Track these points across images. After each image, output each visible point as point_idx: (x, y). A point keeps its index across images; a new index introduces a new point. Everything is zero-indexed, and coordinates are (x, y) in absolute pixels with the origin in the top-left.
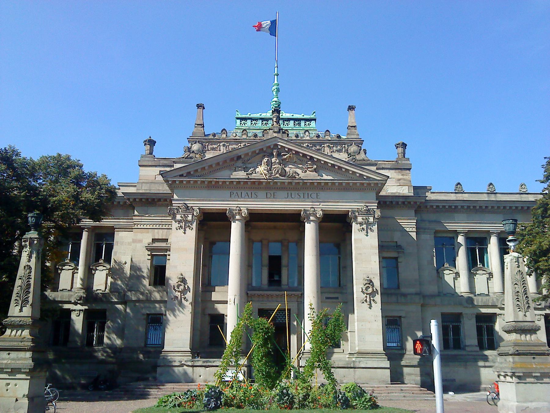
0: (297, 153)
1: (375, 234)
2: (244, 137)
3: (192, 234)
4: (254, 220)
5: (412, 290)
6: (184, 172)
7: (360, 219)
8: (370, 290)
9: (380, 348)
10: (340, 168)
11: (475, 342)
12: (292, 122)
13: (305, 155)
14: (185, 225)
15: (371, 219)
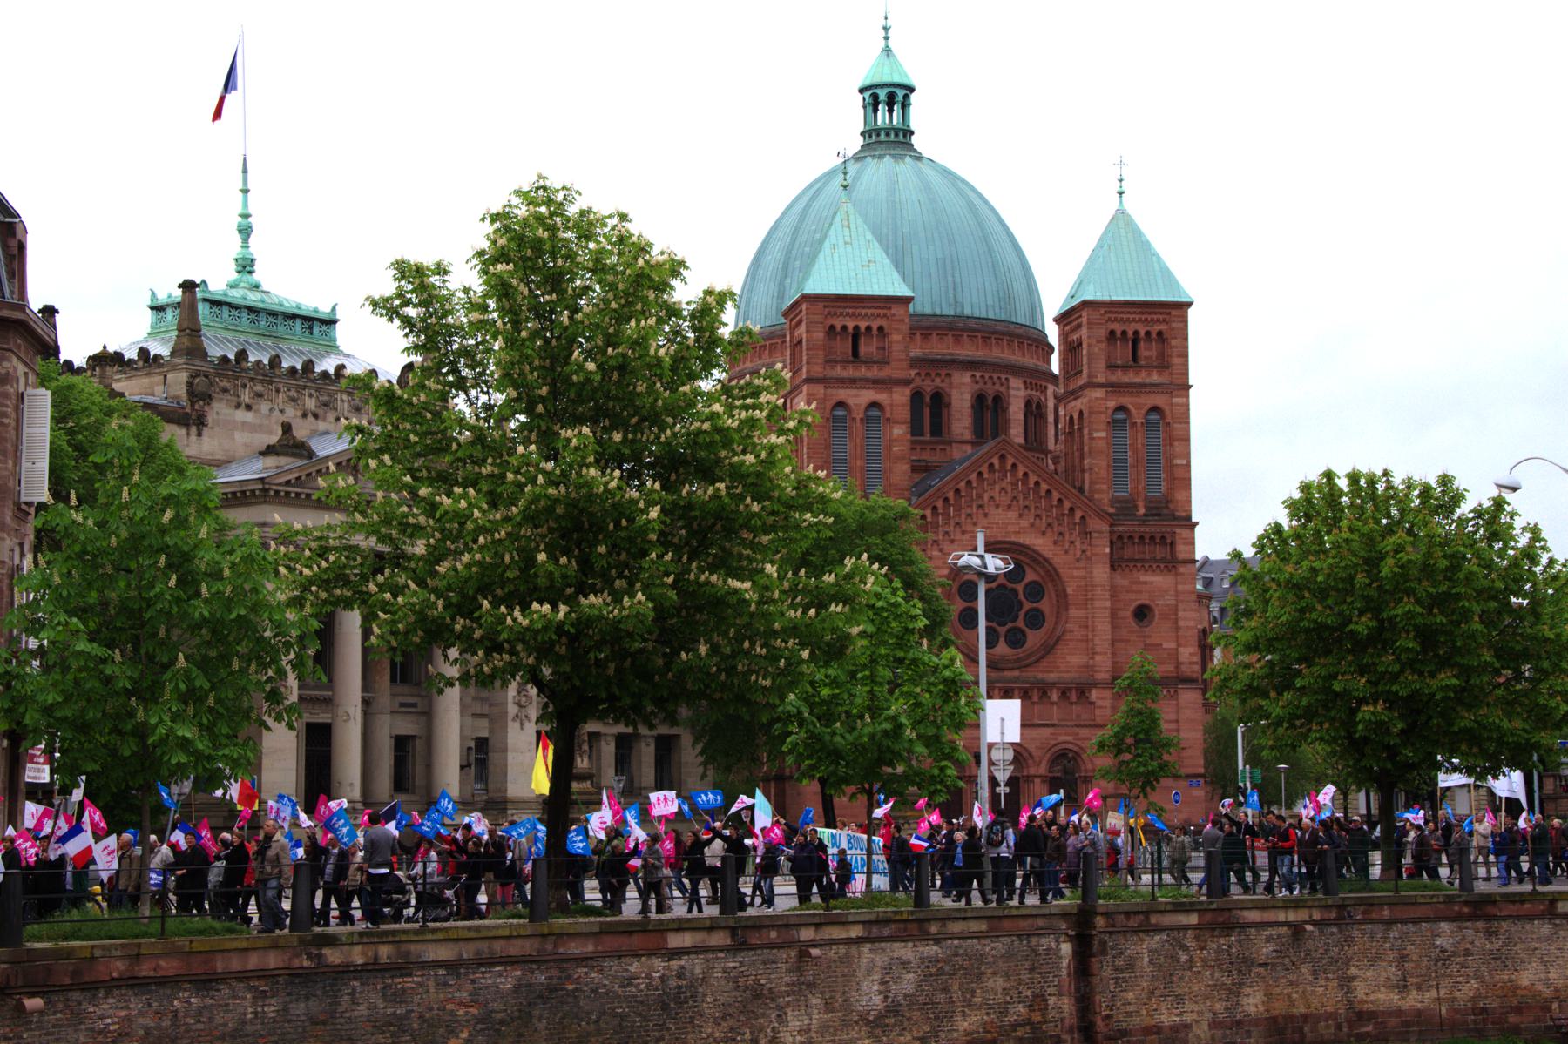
12: (298, 322)
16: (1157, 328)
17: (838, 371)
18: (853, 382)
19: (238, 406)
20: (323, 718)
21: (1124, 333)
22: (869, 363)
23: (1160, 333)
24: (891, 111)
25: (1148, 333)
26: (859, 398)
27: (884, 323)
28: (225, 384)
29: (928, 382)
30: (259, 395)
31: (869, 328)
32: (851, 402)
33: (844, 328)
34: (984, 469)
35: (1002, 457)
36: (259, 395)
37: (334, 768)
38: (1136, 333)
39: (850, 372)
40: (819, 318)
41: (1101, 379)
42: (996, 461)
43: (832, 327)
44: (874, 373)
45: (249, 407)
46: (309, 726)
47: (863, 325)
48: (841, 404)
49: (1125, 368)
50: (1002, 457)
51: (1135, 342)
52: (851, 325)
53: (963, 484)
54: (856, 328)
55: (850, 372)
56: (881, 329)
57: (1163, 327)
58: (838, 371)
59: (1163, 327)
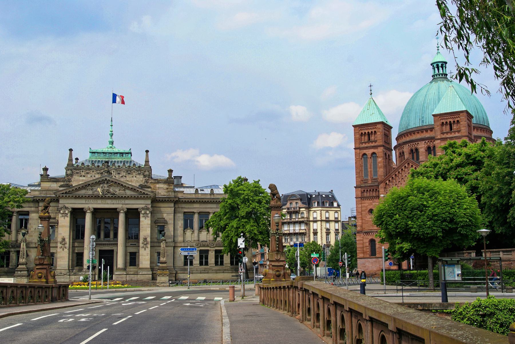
0: (116, 182)
1: (149, 218)
2: (93, 167)
4: (96, 212)
5: (170, 240)
6: (64, 192)
7: (143, 212)
8: (145, 243)
10: (135, 189)
11: (198, 262)
12: (119, 154)
13: (119, 184)
15: (148, 212)
16: (457, 119)
17: (364, 145)
18: (366, 148)
19: (81, 176)
21: (446, 122)
22: (372, 142)
23: (458, 121)
24: (438, 70)
25: (454, 122)
26: (369, 152)
27: (376, 130)
28: (78, 171)
29: (431, 143)
30: (88, 173)
31: (372, 132)
32: (367, 153)
33: (365, 133)
34: (403, 168)
35: (408, 164)
36: (88, 173)
37: (137, 260)
38: (450, 122)
40: (357, 131)
41: (439, 137)
42: (406, 165)
43: (362, 133)
44: (373, 144)
45: (84, 176)
46: (100, 251)
47: (370, 131)
48: (365, 154)
49: (447, 133)
50: (408, 164)
51: (451, 125)
52: (367, 132)
53: (397, 173)
54: (368, 132)
56: (375, 132)
58: (364, 145)
59: (458, 119)
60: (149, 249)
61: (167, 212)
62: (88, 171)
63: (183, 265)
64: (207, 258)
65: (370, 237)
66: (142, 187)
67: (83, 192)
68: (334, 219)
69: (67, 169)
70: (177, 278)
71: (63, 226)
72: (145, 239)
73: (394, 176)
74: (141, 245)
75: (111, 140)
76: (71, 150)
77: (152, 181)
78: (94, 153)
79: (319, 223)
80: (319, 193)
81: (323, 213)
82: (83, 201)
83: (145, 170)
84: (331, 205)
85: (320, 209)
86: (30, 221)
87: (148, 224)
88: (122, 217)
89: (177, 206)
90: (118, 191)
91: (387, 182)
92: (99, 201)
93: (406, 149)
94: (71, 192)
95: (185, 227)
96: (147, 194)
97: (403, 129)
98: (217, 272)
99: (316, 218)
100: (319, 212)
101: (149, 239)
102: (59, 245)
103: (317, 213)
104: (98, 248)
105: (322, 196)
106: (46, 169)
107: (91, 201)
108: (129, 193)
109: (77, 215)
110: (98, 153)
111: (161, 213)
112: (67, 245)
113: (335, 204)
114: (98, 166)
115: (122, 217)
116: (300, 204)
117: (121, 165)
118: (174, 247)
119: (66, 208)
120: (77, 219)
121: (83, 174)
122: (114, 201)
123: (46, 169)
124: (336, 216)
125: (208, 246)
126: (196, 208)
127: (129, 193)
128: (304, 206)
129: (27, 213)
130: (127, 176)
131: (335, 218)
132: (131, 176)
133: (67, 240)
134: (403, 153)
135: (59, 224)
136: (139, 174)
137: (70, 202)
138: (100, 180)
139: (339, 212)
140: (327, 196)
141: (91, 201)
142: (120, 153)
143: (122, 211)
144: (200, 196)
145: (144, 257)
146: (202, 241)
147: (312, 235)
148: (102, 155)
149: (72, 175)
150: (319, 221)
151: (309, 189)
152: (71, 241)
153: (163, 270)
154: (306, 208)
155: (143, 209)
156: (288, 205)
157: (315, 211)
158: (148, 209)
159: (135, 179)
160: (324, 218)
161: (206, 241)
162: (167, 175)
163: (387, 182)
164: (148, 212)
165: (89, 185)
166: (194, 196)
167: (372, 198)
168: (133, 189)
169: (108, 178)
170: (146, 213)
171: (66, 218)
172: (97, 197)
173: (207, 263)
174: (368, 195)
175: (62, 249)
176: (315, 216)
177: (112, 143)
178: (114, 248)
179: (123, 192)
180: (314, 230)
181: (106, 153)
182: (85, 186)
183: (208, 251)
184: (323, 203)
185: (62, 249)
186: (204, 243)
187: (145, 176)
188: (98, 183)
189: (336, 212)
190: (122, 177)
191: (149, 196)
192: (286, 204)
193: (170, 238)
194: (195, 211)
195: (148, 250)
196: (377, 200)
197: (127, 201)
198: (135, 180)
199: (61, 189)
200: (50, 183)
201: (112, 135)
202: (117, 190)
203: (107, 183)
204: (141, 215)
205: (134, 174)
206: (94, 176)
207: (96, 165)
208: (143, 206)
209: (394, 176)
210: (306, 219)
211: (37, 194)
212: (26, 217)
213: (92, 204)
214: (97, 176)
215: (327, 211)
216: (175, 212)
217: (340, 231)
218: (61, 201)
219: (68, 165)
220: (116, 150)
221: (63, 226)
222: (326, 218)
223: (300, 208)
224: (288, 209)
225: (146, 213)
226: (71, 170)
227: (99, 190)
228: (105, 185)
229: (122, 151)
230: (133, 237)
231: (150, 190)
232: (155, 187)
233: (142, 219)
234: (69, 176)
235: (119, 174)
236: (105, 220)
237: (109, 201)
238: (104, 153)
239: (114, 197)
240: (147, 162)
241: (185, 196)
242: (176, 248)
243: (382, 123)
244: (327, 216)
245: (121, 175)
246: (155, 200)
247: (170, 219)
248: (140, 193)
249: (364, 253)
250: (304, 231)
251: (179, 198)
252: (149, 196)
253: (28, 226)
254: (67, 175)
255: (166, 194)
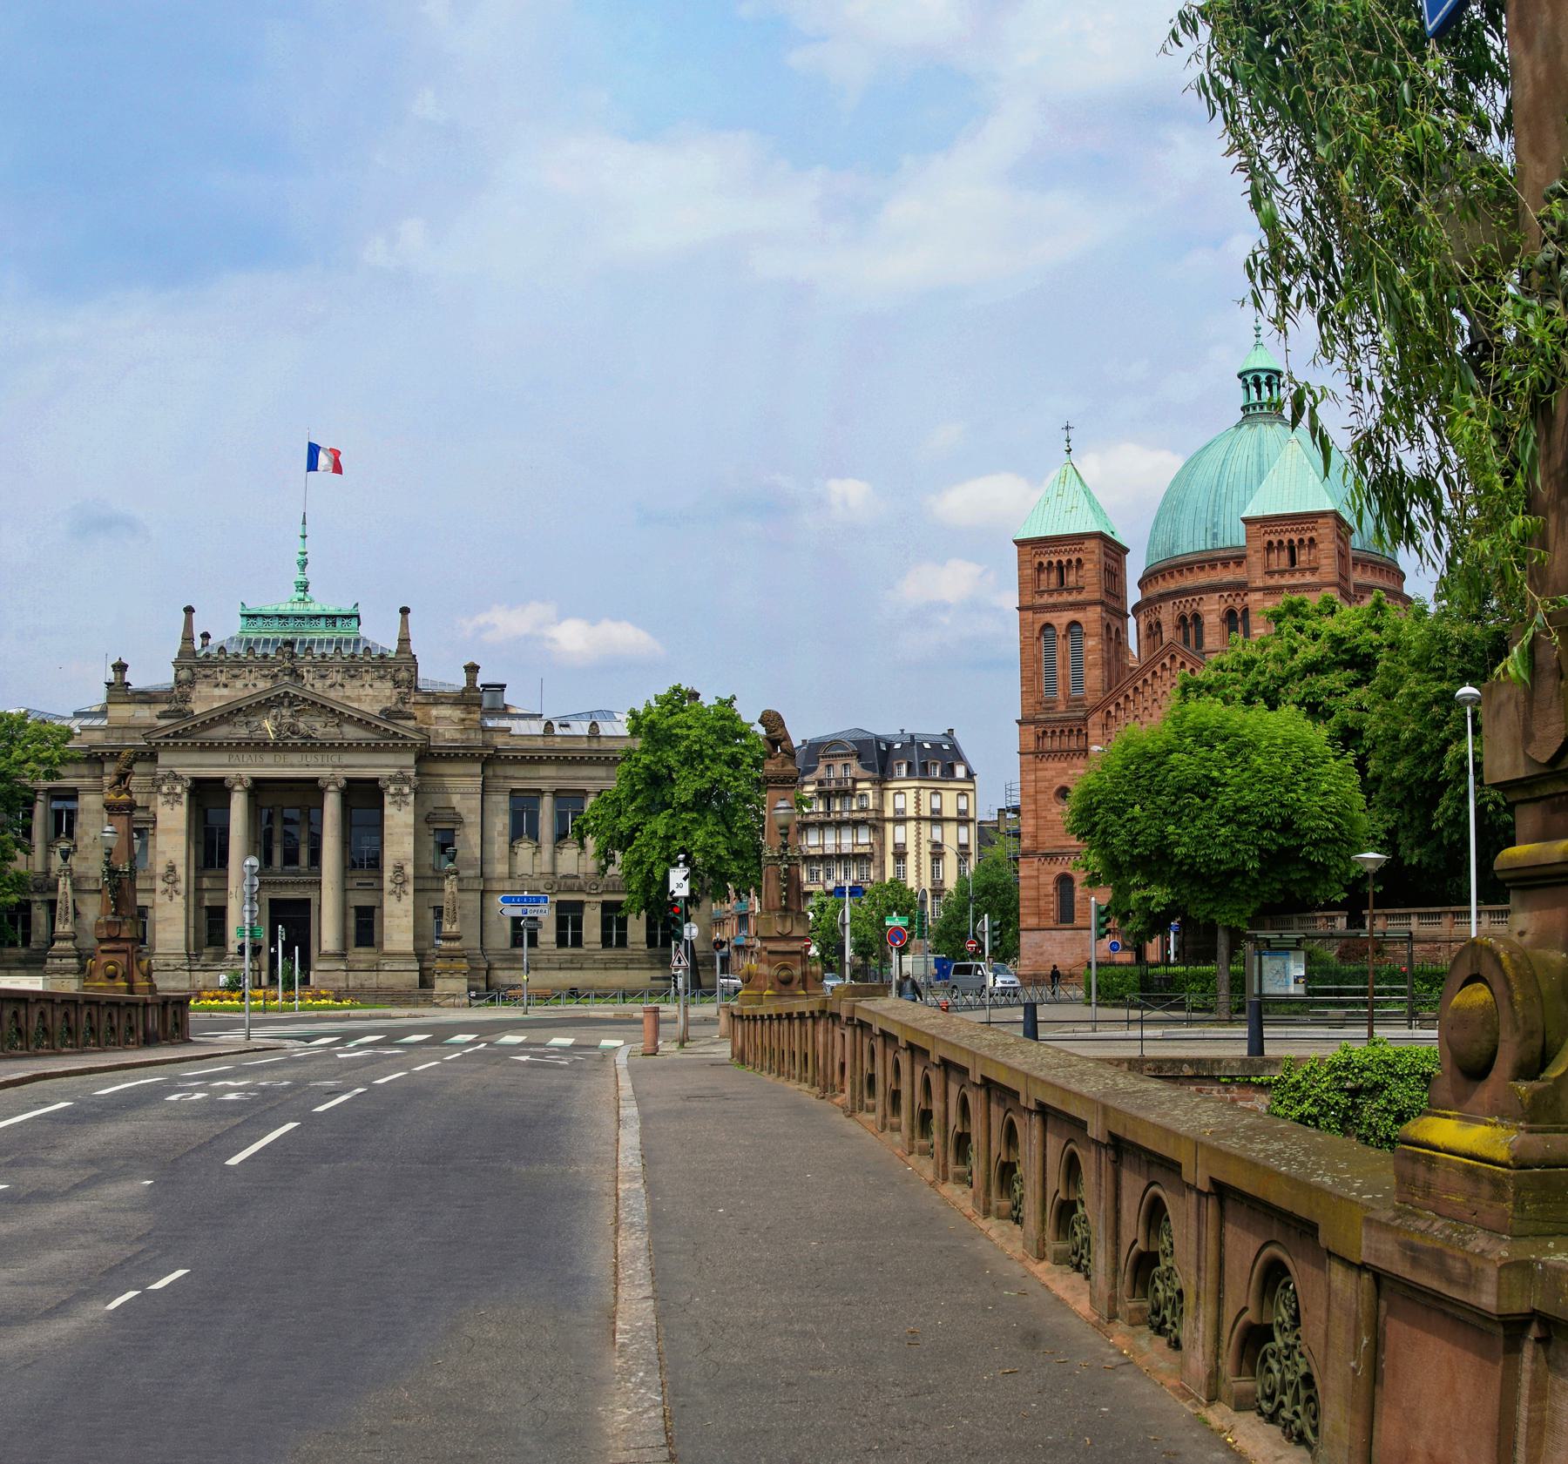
0: (314, 703)
1: (411, 808)
3: (181, 811)
4: (258, 788)
7: (392, 790)
9: (410, 948)
10: (368, 723)
11: (553, 938)
12: (323, 621)
14: (173, 798)
15: (406, 790)
18: (1054, 607)
19: (217, 686)
20: (51, 896)
22: (1070, 590)
26: (1061, 619)
27: (1081, 555)
28: (208, 672)
30: (235, 676)
31: (1069, 561)
32: (1054, 622)
33: (1050, 563)
34: (1158, 668)
36: (235, 676)
37: (376, 929)
39: (1055, 599)
40: (1027, 558)
43: (1041, 564)
45: (226, 686)
46: (271, 901)
47: (1064, 559)
48: (1048, 626)
52: (1055, 561)
54: (1060, 562)
55: (1055, 599)
56: (1079, 561)
57: (1314, 534)
58: (1047, 599)
60: (411, 897)
61: (461, 790)
62: (236, 672)
63: (508, 945)
64: (578, 925)
65: (1058, 869)
66: (389, 714)
67: (221, 732)
68: (954, 815)
69: (179, 665)
70: (492, 982)
71: (168, 831)
72: (399, 869)
73: (1130, 692)
74: (388, 886)
75: (300, 578)
76: (189, 610)
77: (419, 698)
78: (254, 616)
79: (912, 825)
80: (912, 737)
81: (925, 794)
82: (223, 758)
83: (399, 667)
84: (949, 773)
85: (916, 784)
86: (81, 817)
87: (406, 826)
88: (331, 805)
89: (490, 772)
90: (320, 728)
91: (1112, 708)
92: (269, 758)
93: (1167, 614)
94: (189, 732)
95: (515, 835)
96: (404, 737)
97: (1160, 557)
98: (607, 966)
99: (903, 811)
100: (911, 794)
101: (409, 870)
102: (160, 885)
103: (905, 796)
104: (267, 895)
105: (921, 745)
106: (120, 668)
107: (246, 757)
108: (351, 733)
109: (207, 797)
110: (264, 616)
111: (444, 791)
112: (182, 886)
113: (960, 772)
114: (265, 656)
115: (331, 805)
116: (855, 768)
117: (330, 651)
118: (483, 893)
119: (177, 778)
120: (206, 811)
121: (222, 679)
122: (311, 758)
123: (120, 668)
124: (963, 806)
125: (581, 890)
126: (547, 778)
127: (351, 733)
128: (869, 774)
129: (73, 794)
130: (346, 682)
131: (960, 812)
132: (359, 683)
133: (181, 871)
134: (1159, 625)
135: (159, 825)
136: (381, 678)
137: (188, 762)
138: (271, 695)
139: (971, 795)
140: (936, 747)
141: (246, 756)
142: (328, 617)
143: (332, 788)
144: (558, 743)
145: (397, 921)
146: (565, 877)
147: (889, 860)
148: (276, 622)
149: (191, 683)
150: (911, 819)
151: (885, 725)
152: (192, 874)
153: (452, 958)
154: (873, 781)
155: (392, 779)
156: (821, 772)
157: (900, 791)
158: (405, 780)
159: (369, 691)
160: (926, 812)
161: (576, 877)
162: (461, 681)
163: (1112, 708)
164: (406, 790)
165: (240, 710)
166: (540, 743)
167: (1067, 754)
168: (362, 722)
169: (292, 691)
170: (400, 793)
171: (177, 807)
172: (262, 746)
173: (578, 941)
174: (1056, 745)
175: (166, 897)
176: (900, 805)
177: (304, 587)
178: (311, 894)
179: (335, 730)
180: (895, 845)
181: (286, 617)
182: (229, 714)
183: (581, 904)
184: (924, 767)
185: (166, 897)
186: (569, 882)
187: (397, 684)
188: (265, 705)
189: (963, 793)
190: (331, 686)
191: (409, 743)
192: (815, 769)
193: (470, 866)
194: (543, 788)
195: (408, 900)
196: (1081, 762)
197: (347, 758)
198: (371, 697)
199: (163, 723)
200: (132, 707)
201: (304, 565)
202: (318, 726)
203: (291, 704)
204: (387, 799)
205: (367, 677)
206: (255, 685)
207: (259, 651)
208: (393, 771)
209: (1130, 692)
210: (872, 815)
211: (97, 737)
212: (70, 805)
213: (248, 766)
214: (263, 685)
215: (936, 792)
216: (484, 792)
217: (972, 849)
218: (163, 759)
219: (180, 653)
220: (315, 609)
221: (168, 831)
222: (933, 811)
223: (855, 781)
224: (821, 783)
225: (400, 793)
226: (190, 668)
227: (268, 724)
228: (284, 712)
229: (331, 611)
230: (363, 861)
231: (411, 723)
232: (427, 715)
233: (389, 810)
234: (184, 686)
235: (323, 677)
236: (284, 812)
237: (295, 758)
238: (280, 617)
239: (311, 745)
240: (404, 641)
241: (513, 743)
242: (488, 896)
243: (1100, 536)
244: (936, 805)
245: (329, 682)
246: (427, 756)
247: (470, 811)
248: (383, 733)
249: (1039, 915)
250: (867, 849)
251: (497, 750)
252: (409, 743)
253: (77, 830)
254: (178, 682)
255: (458, 736)
